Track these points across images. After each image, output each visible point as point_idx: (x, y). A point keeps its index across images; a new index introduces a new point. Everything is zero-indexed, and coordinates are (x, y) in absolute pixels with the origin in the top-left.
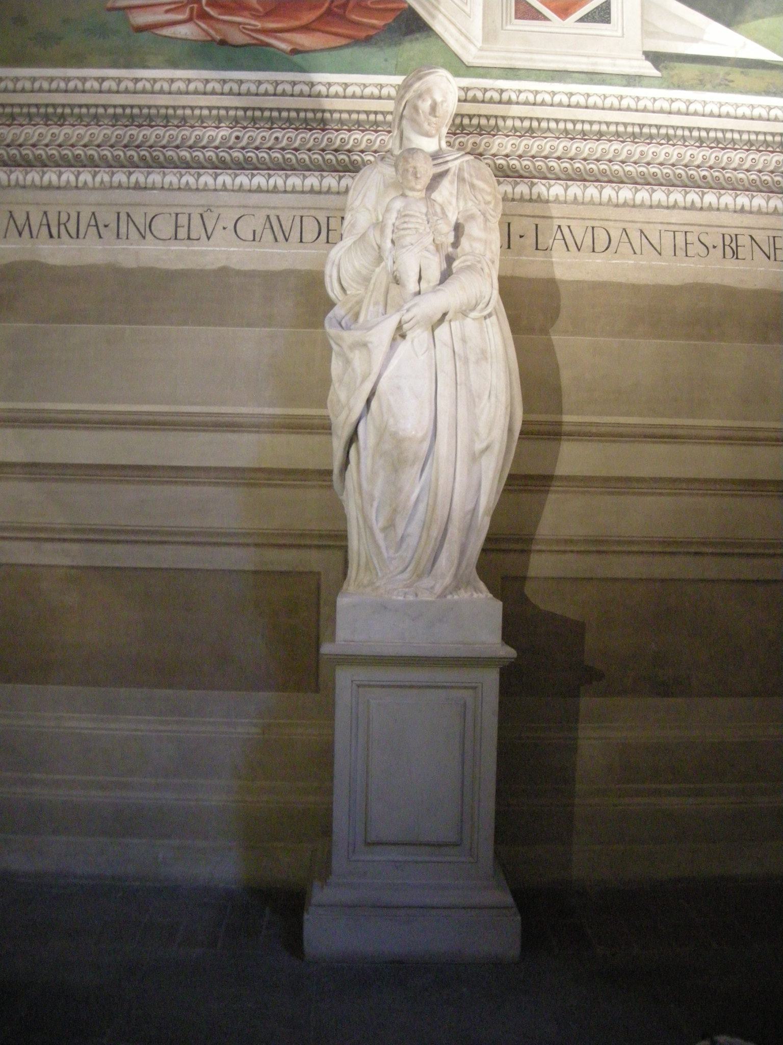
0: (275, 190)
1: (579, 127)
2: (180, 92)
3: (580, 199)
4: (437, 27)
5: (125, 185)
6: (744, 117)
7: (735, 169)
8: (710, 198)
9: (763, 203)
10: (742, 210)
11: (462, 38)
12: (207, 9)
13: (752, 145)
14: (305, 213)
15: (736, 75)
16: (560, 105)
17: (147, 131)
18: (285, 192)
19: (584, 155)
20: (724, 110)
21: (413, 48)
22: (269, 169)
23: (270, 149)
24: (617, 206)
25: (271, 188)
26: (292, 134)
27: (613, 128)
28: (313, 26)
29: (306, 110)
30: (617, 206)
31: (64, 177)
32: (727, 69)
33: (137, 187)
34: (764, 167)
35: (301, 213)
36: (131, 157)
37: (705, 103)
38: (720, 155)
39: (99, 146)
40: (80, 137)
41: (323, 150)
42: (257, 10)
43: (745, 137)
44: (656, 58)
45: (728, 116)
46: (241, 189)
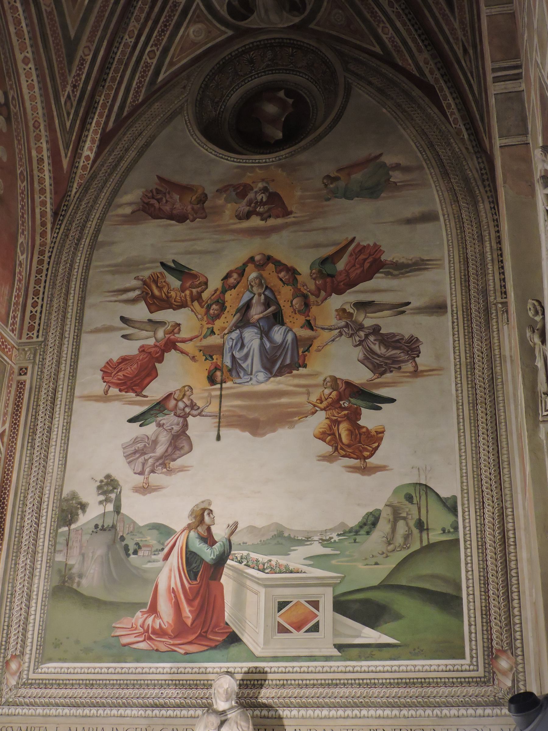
0: (176, 717)
1: (304, 682)
2: (139, 673)
3: (305, 716)
4: (244, 640)
5: (116, 715)
6: (380, 672)
7: (376, 697)
8: (364, 712)
9: (389, 713)
10: (379, 717)
11: (255, 644)
12: (151, 636)
13: (384, 685)
14: (188, 727)
15: (376, 652)
16: (296, 672)
17: (126, 691)
18: (180, 717)
19: (307, 695)
20: (370, 669)
21: (234, 649)
22: (174, 707)
23: (175, 698)
24: (321, 718)
25: (175, 716)
26: (184, 691)
27: (319, 682)
28: (193, 642)
29: (190, 680)
30: (321, 718)
31: (92, 712)
32: (372, 649)
33: (121, 716)
34: (390, 695)
35: (185, 727)
36: (119, 702)
37: (361, 667)
38: (369, 691)
39: (106, 698)
40: (99, 694)
41: (196, 698)
42: (171, 635)
43: (380, 681)
44: (339, 647)
45: (372, 672)
46: (162, 717)
